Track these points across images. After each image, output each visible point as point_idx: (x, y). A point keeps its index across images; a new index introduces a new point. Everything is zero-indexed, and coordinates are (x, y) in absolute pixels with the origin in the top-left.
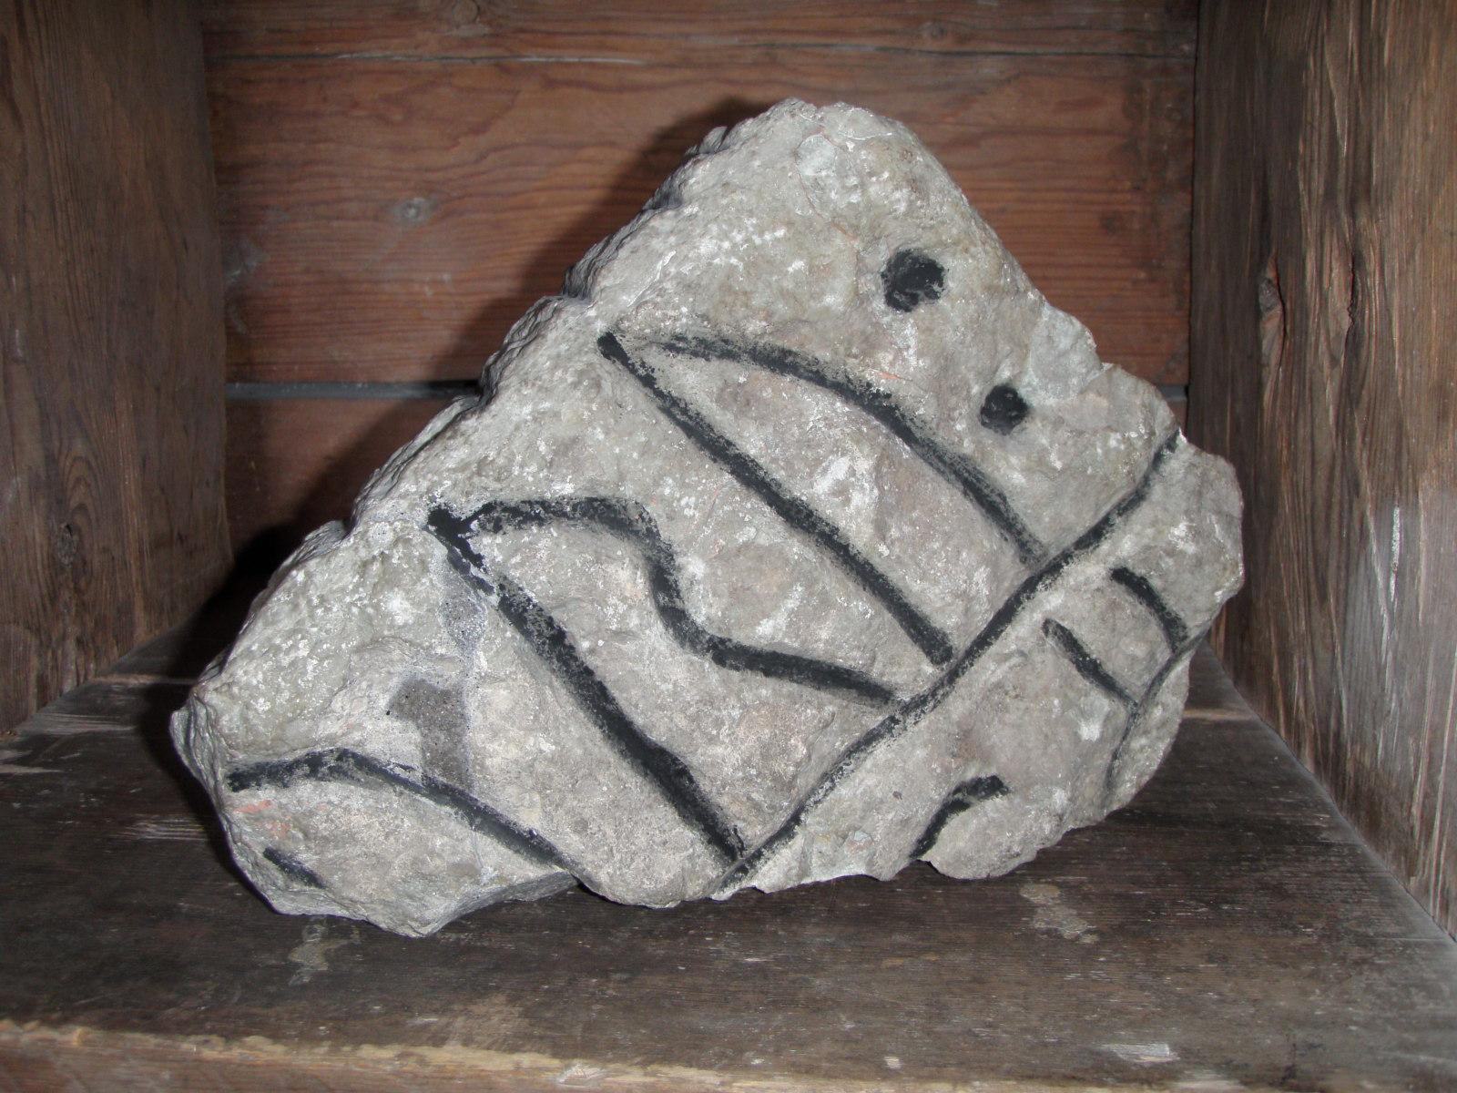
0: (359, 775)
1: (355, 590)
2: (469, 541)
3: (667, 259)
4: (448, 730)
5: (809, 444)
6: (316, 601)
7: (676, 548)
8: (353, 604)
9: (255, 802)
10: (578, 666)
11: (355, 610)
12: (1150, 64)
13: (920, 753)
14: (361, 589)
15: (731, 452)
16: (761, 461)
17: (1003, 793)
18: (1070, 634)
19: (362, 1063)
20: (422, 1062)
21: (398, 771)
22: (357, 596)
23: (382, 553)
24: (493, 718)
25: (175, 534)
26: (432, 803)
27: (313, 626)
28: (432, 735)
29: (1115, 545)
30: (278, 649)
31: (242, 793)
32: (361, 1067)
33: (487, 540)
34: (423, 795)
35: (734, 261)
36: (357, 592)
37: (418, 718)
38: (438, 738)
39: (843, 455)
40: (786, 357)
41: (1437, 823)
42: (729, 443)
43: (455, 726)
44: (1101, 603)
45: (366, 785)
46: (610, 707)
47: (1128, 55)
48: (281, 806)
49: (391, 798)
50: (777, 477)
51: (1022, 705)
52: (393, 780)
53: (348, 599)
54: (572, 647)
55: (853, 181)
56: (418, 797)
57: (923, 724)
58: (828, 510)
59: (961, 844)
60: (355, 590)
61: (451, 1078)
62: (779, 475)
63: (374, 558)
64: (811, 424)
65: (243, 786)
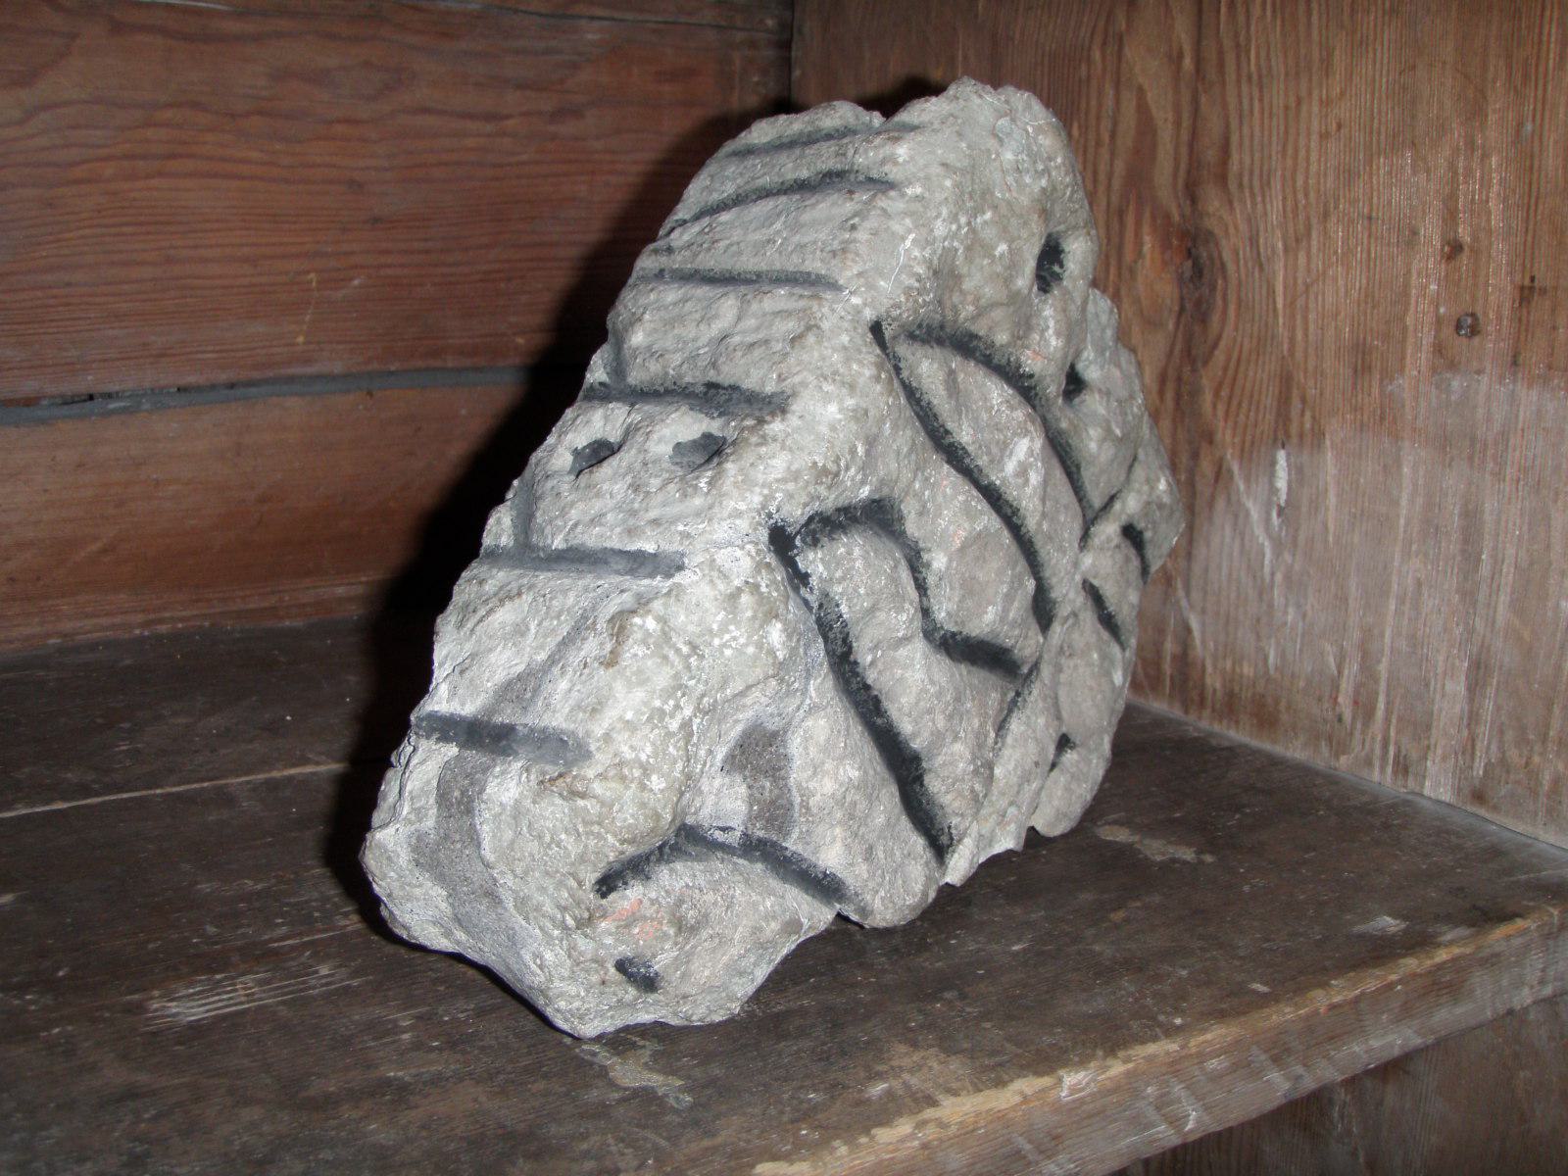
0: (691, 849)
1: (724, 629)
2: (797, 558)
3: (908, 243)
4: (773, 776)
5: (998, 428)
6: (685, 649)
7: (921, 545)
8: (724, 645)
9: (626, 904)
10: (858, 683)
11: (728, 652)
12: (740, 36)
13: (1041, 721)
14: (732, 628)
15: (948, 440)
16: (970, 449)
17: (1071, 748)
18: (1097, 591)
19: (891, 1147)
20: (942, 1124)
21: (719, 836)
22: (727, 637)
23: (747, 582)
24: (813, 751)
25: (508, 588)
26: (746, 863)
27: (691, 678)
28: (757, 785)
29: (1124, 503)
30: (662, 713)
31: (612, 896)
32: (891, 1152)
33: (811, 555)
34: (739, 856)
35: (956, 244)
36: (728, 631)
37: (746, 768)
38: (763, 787)
39: (1025, 436)
40: (971, 341)
41: (1381, 706)
42: (947, 432)
43: (780, 769)
44: (1119, 557)
45: (698, 859)
46: (879, 721)
47: (718, 27)
48: (653, 902)
49: (720, 867)
50: (980, 463)
51: (1071, 663)
52: (716, 846)
53: (717, 642)
54: (856, 663)
55: (1040, 167)
56: (735, 859)
57: (1035, 692)
58: (1012, 494)
59: (1056, 803)
60: (724, 629)
61: (973, 1131)
62: (982, 461)
63: (739, 590)
64: (996, 408)
65: (611, 889)
